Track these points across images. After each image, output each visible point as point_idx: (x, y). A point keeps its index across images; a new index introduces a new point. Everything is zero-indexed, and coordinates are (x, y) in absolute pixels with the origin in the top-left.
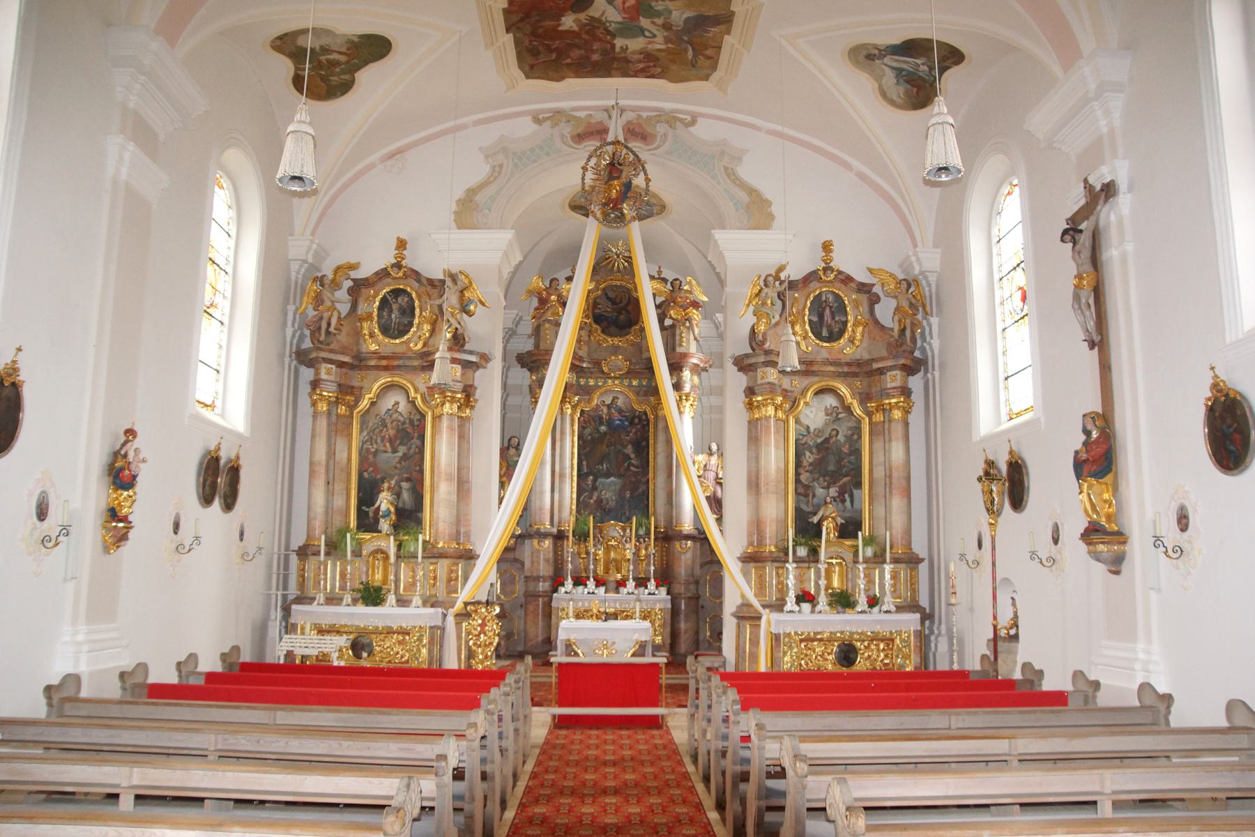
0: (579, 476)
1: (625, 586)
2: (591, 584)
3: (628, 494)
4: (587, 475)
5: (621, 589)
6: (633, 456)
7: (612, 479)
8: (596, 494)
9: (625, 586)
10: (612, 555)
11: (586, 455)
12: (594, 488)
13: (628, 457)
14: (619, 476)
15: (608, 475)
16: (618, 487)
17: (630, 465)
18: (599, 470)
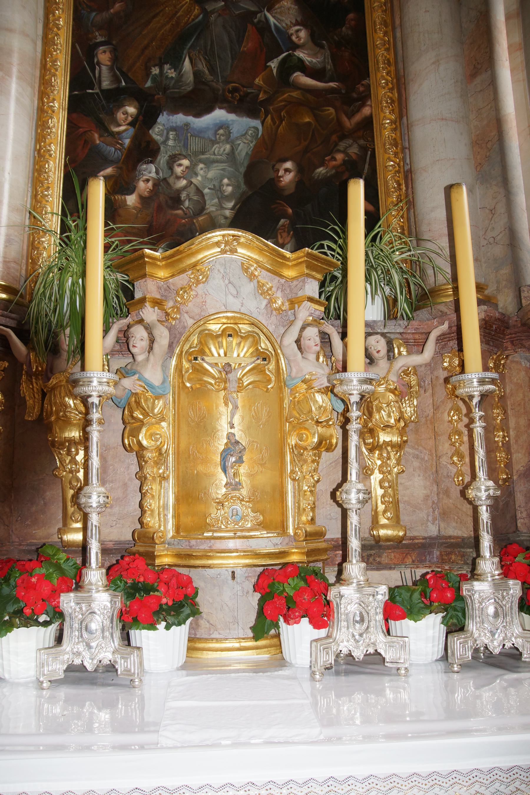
0: (76, 105)
1: (321, 614)
2: (98, 601)
3: (287, 174)
4: (115, 98)
5: (299, 636)
6: (302, 35)
7: (219, 114)
8: (149, 172)
9: (321, 614)
10: (230, 421)
11: (111, 28)
12: (145, 149)
13: (274, 42)
14: (244, 104)
15: (198, 101)
16: (244, 149)
17: (291, 66)
18: (161, 84)
